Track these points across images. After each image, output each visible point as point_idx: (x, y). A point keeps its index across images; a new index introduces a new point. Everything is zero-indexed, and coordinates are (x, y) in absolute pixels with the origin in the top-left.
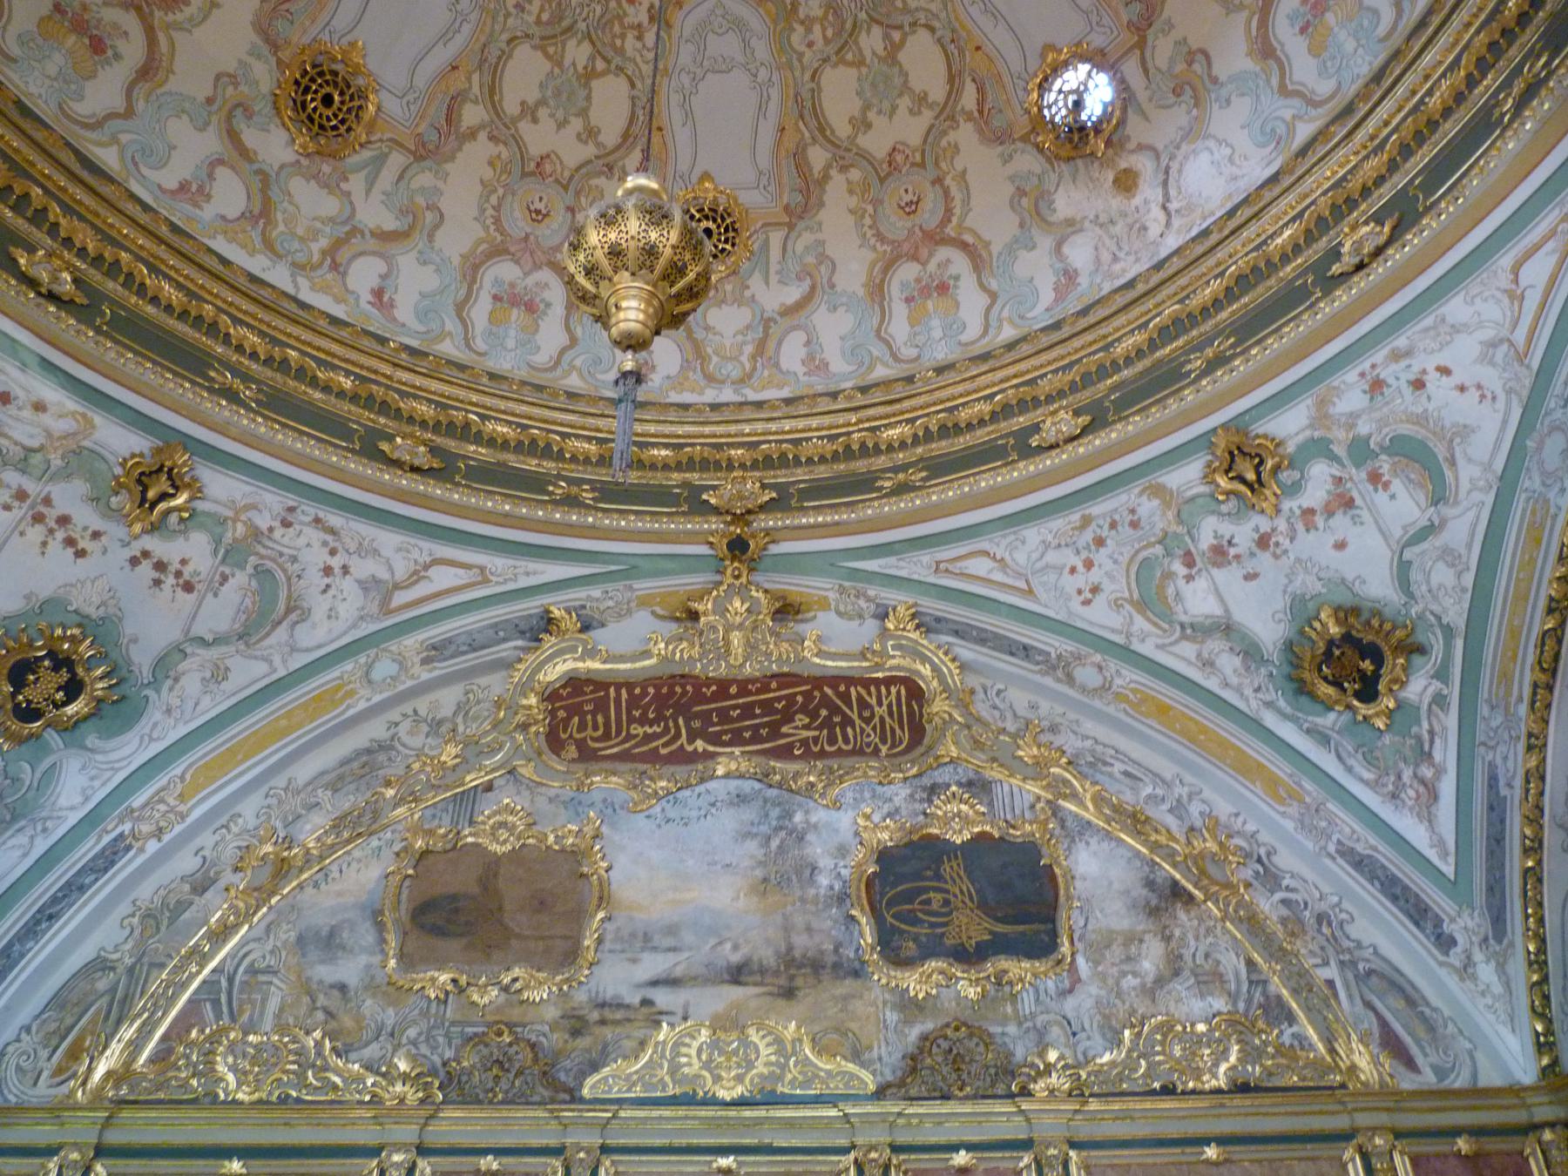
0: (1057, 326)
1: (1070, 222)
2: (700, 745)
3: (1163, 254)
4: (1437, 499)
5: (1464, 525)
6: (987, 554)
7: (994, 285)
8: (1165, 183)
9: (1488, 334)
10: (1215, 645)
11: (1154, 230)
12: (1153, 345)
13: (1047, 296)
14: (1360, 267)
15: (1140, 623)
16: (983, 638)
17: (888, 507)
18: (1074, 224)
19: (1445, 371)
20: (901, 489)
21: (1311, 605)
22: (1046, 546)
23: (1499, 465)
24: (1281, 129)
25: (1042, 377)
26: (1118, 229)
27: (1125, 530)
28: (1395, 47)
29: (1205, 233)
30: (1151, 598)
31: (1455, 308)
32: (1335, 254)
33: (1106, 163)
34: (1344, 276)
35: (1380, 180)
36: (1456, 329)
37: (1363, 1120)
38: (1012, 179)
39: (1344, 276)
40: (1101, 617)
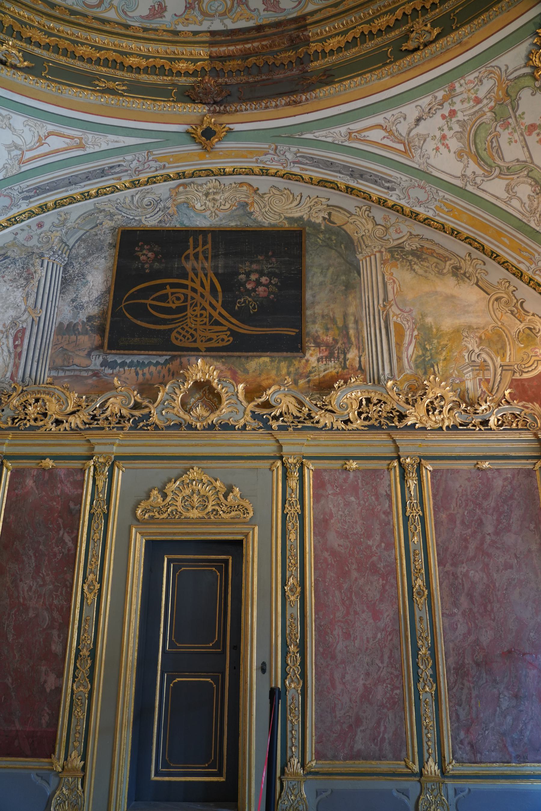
9: (19, 142)
28: (87, 13)
31: (18, 121)
35: (38, 45)
36: (10, 127)
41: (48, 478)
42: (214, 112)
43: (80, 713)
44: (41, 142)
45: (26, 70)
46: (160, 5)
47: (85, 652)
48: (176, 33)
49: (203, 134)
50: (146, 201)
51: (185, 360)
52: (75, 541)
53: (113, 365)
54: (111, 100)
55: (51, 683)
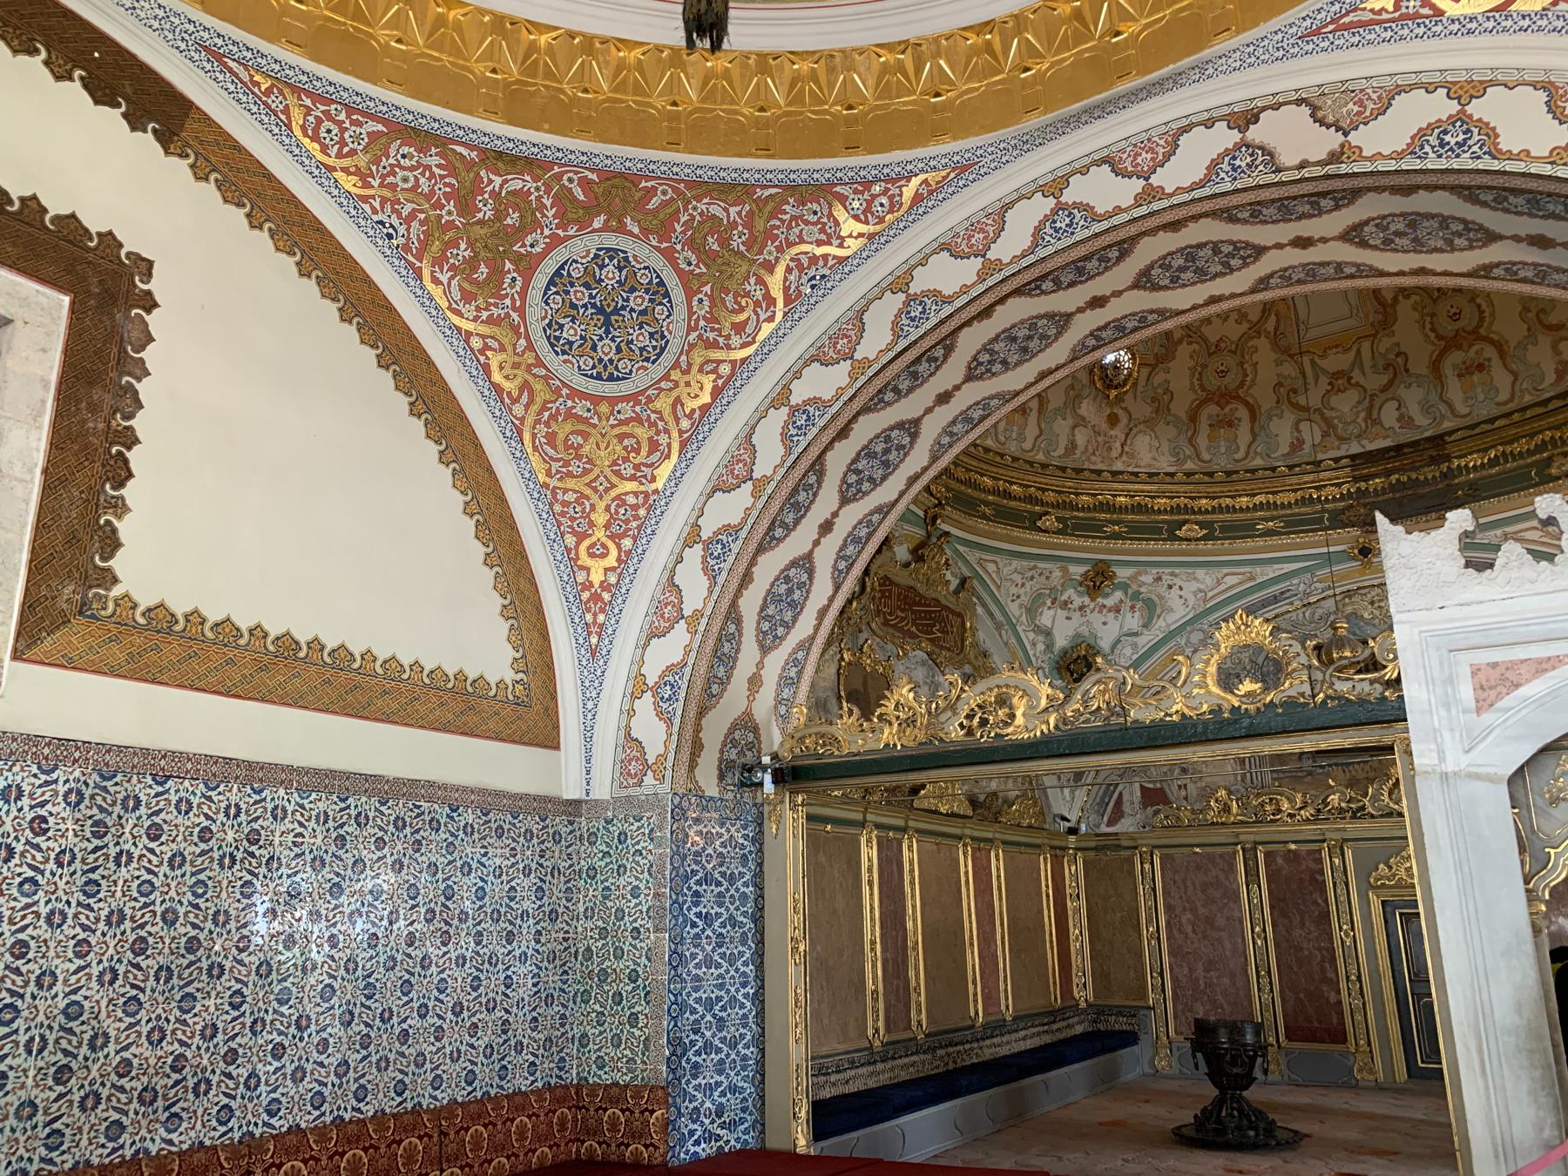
0: (1063, 469)
1: (1083, 419)
3: (1114, 468)
4: (1145, 626)
5: (1146, 640)
10: (1041, 638)
11: (1114, 454)
13: (1061, 451)
16: (984, 605)
17: (982, 524)
18: (1081, 422)
20: (984, 517)
22: (1016, 570)
26: (1100, 439)
29: (1136, 474)
31: (1200, 573)
33: (1111, 404)
35: (1207, 512)
40: (1014, 609)
43: (1359, 1017)
45: (1204, 538)
49: (1360, 552)
50: (1317, 616)
52: (1326, 901)
55: (1333, 998)
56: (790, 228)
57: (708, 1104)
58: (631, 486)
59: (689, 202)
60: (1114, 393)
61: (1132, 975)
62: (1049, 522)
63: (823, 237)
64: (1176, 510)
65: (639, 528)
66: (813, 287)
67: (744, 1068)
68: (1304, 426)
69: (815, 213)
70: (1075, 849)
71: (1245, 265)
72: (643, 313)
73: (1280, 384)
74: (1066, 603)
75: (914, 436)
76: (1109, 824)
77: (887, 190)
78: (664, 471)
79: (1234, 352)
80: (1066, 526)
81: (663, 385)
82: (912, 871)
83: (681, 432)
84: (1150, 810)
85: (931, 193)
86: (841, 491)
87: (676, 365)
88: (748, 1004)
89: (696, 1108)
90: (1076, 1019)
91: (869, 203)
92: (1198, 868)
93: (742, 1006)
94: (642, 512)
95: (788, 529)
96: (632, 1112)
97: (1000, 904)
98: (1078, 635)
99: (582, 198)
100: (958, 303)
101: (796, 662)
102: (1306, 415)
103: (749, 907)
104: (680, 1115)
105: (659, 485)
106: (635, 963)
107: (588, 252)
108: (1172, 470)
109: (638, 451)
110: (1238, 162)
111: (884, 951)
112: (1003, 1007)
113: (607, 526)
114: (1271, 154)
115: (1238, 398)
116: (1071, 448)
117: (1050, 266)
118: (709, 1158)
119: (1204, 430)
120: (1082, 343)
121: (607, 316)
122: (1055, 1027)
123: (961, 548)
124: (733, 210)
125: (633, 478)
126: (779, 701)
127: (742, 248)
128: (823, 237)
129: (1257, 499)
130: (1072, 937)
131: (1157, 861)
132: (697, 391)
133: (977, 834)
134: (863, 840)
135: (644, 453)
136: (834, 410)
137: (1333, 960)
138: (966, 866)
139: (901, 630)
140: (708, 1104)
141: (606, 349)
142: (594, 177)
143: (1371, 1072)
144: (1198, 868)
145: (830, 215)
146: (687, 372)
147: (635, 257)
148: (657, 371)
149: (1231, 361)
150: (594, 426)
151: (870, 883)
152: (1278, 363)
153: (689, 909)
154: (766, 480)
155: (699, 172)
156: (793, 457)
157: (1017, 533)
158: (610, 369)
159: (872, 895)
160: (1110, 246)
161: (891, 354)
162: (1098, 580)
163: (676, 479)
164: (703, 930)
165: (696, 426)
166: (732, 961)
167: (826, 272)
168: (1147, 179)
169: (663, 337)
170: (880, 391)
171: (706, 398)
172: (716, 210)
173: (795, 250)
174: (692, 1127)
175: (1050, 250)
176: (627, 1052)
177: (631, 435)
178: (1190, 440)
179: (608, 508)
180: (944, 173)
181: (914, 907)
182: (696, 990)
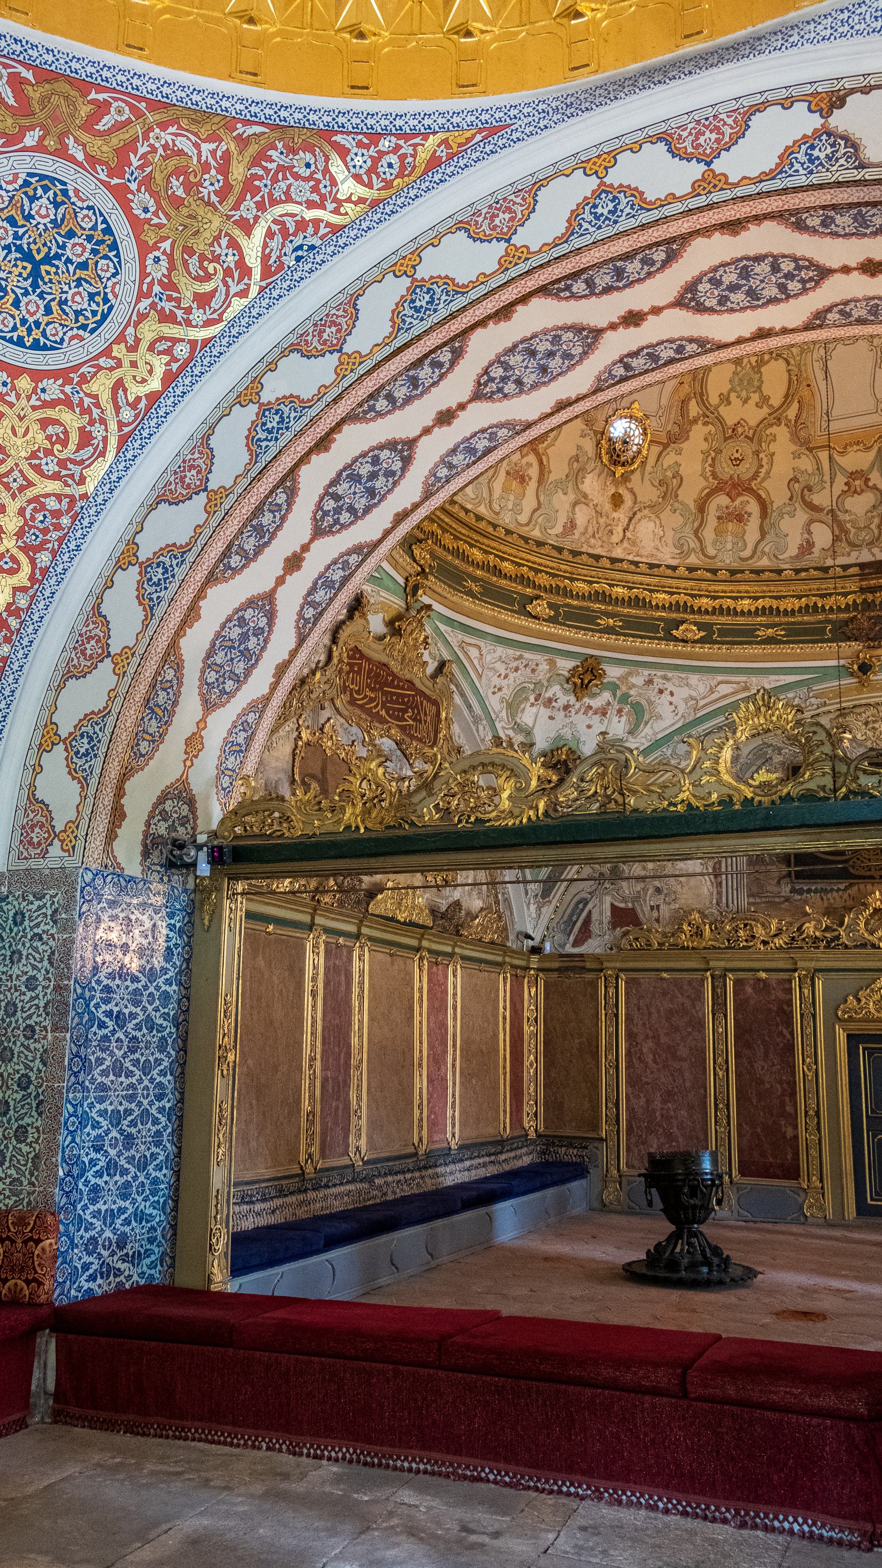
0: (560, 550)
1: (585, 496)
2: (383, 713)
3: (614, 555)
6: (479, 648)
7: (542, 499)
8: (631, 519)
9: (694, 694)
11: (615, 538)
12: (590, 597)
13: (558, 529)
14: (685, 641)
15: (504, 714)
16: (462, 695)
17: (468, 603)
18: (583, 499)
19: (672, 694)
20: (470, 593)
21: (562, 743)
23: (660, 736)
24: (685, 548)
25: (541, 571)
26: (602, 521)
27: (529, 670)
29: (636, 564)
30: (513, 706)
31: (694, 679)
32: (678, 624)
33: (616, 483)
34: (676, 639)
35: (707, 612)
36: (687, 685)
37: (507, 959)
38: (579, 448)
39: (676, 639)
40: (494, 703)
41: (763, 987)
42: (869, 647)
43: (814, 1153)
44: (712, 691)
45: (701, 641)
46: (808, 542)
47: (811, 1112)
48: (825, 570)
49: (860, 668)
51: (862, 886)
53: (800, 892)
54: (770, 649)
55: (790, 1132)
56: (275, 180)
57: (108, 1234)
58: (54, 486)
59: (150, 129)
60: (620, 470)
61: (587, 1105)
62: (540, 607)
63: (316, 197)
64: (676, 607)
65: (60, 540)
66: (298, 259)
67: (154, 1193)
68: (816, 527)
69: (308, 165)
70: (539, 970)
71: (805, 291)
72: (83, 266)
73: (795, 480)
74: (550, 700)
75: (407, 461)
76: (574, 946)
77: (398, 147)
78: (96, 472)
79: (751, 439)
80: (557, 614)
81: (102, 362)
82: (361, 984)
83: (121, 425)
84: (618, 931)
85: (450, 157)
86: (314, 518)
87: (121, 338)
88: (163, 1120)
89: (93, 1238)
90: (524, 1150)
91: (376, 161)
92: (664, 994)
93: (156, 1122)
94: (65, 521)
95: (249, 559)
96: (13, 1242)
97: (454, 1024)
98: (559, 737)
99: (11, 101)
100: (473, 295)
101: (245, 726)
102: (816, 515)
103: (171, 1009)
104: (73, 1246)
105: (90, 487)
106: (27, 1067)
107: (16, 176)
108: (674, 563)
109: (65, 443)
110: (816, 153)
111: (325, 1068)
112: (449, 1135)
113: (20, 534)
114: (855, 146)
115: (751, 491)
116: (571, 525)
117: (586, 260)
118: (105, 1296)
119: (712, 522)
120: (609, 370)
121: (36, 265)
122: (503, 1157)
123: (443, 627)
124: (206, 147)
125: (56, 476)
126: (222, 771)
127: (214, 199)
128: (316, 197)
129: (760, 603)
130: (527, 1063)
131: (622, 985)
132: (145, 375)
133: (435, 947)
134: (309, 946)
135: (72, 446)
136: (313, 412)
137: (793, 1094)
138: (421, 980)
139: (369, 712)
140: (108, 1234)
141: (32, 305)
142: (28, 75)
143: (821, 1208)
144: (664, 994)
145: (326, 171)
146: (133, 349)
147: (77, 191)
148: (95, 343)
149: (747, 449)
150: (11, 405)
151: (314, 994)
152: (796, 456)
153: (97, 1006)
154: (226, 491)
155: (165, 90)
156: (259, 466)
157: (504, 616)
158: (36, 334)
159: (314, 1006)
160: (658, 244)
161: (388, 350)
162: (586, 677)
163: (111, 483)
164: (114, 1032)
165: (140, 418)
166: (146, 1069)
167: (317, 242)
168: (708, 164)
169: (106, 300)
170: (371, 396)
171: (155, 384)
172: (183, 143)
173: (279, 210)
174: (87, 1259)
175: (588, 240)
176: (12, 1172)
177: (57, 422)
178: (696, 532)
179: (21, 512)
180: (468, 134)
181: (361, 1022)
182: (101, 1100)
